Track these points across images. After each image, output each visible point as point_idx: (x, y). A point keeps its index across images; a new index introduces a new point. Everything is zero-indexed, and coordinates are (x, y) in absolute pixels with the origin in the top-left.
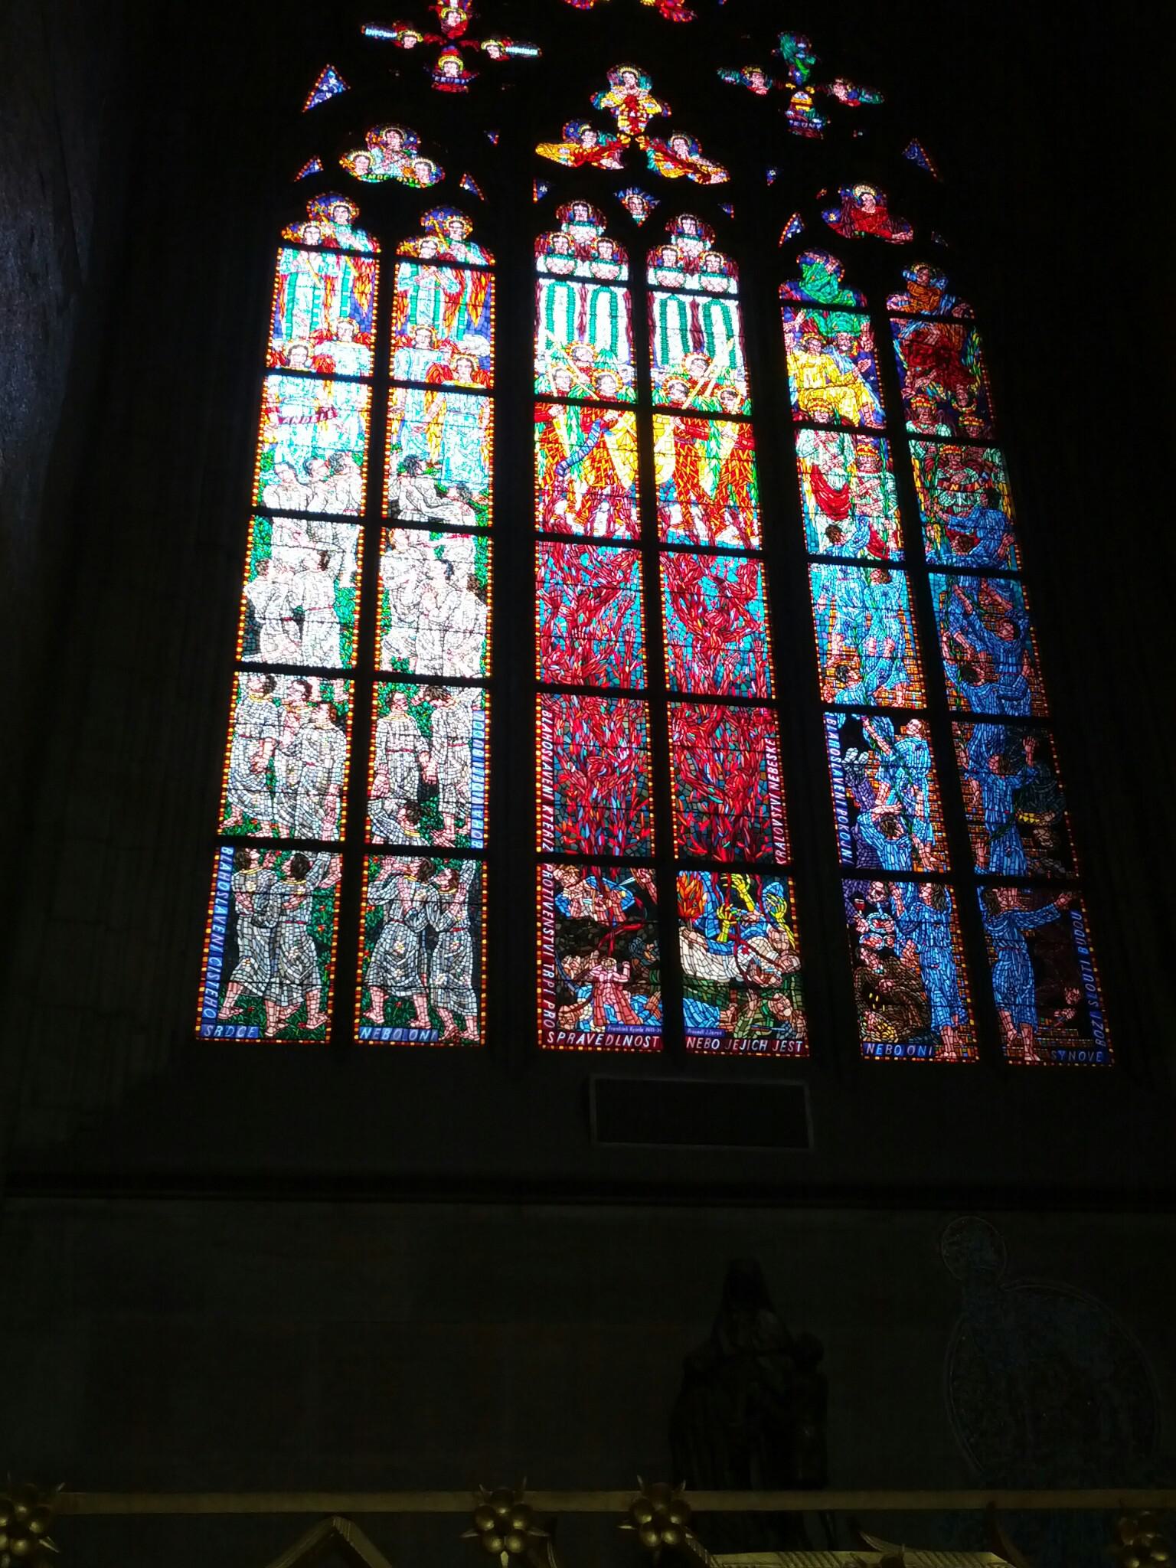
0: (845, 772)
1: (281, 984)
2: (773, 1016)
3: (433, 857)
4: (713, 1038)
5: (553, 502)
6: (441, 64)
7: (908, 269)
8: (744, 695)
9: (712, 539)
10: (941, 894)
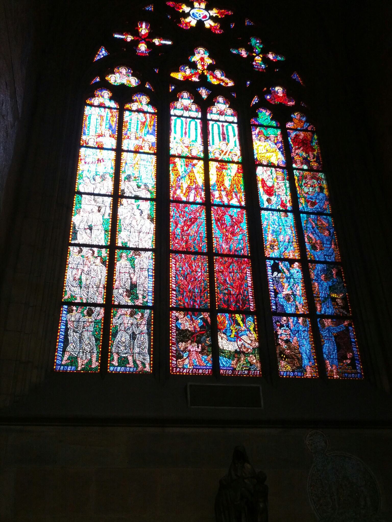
0: (273, 280)
1: (83, 352)
2: (249, 362)
3: (135, 308)
4: (229, 370)
5: (176, 190)
6: (139, 46)
7: (293, 114)
8: (240, 254)
9: (229, 202)
10: (306, 321)
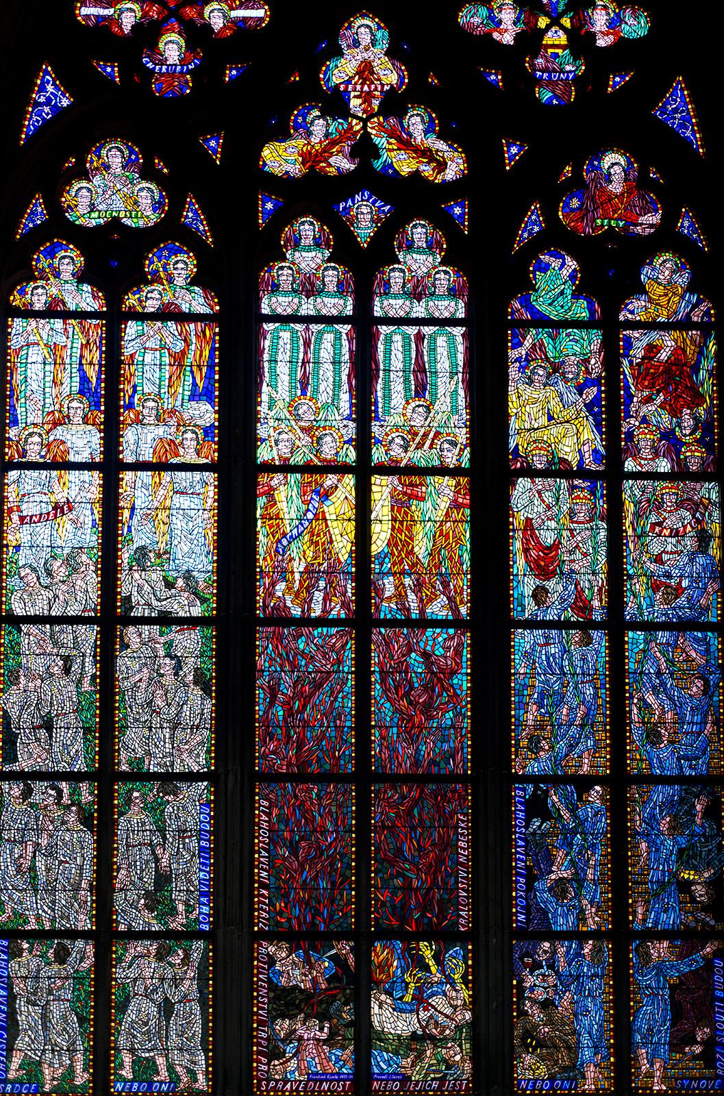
1: (53, 1050)
2: (445, 1061)
4: (394, 1081)
5: (273, 584)
6: (161, 45)
8: (442, 772)
9: (422, 611)
10: (600, 950)
